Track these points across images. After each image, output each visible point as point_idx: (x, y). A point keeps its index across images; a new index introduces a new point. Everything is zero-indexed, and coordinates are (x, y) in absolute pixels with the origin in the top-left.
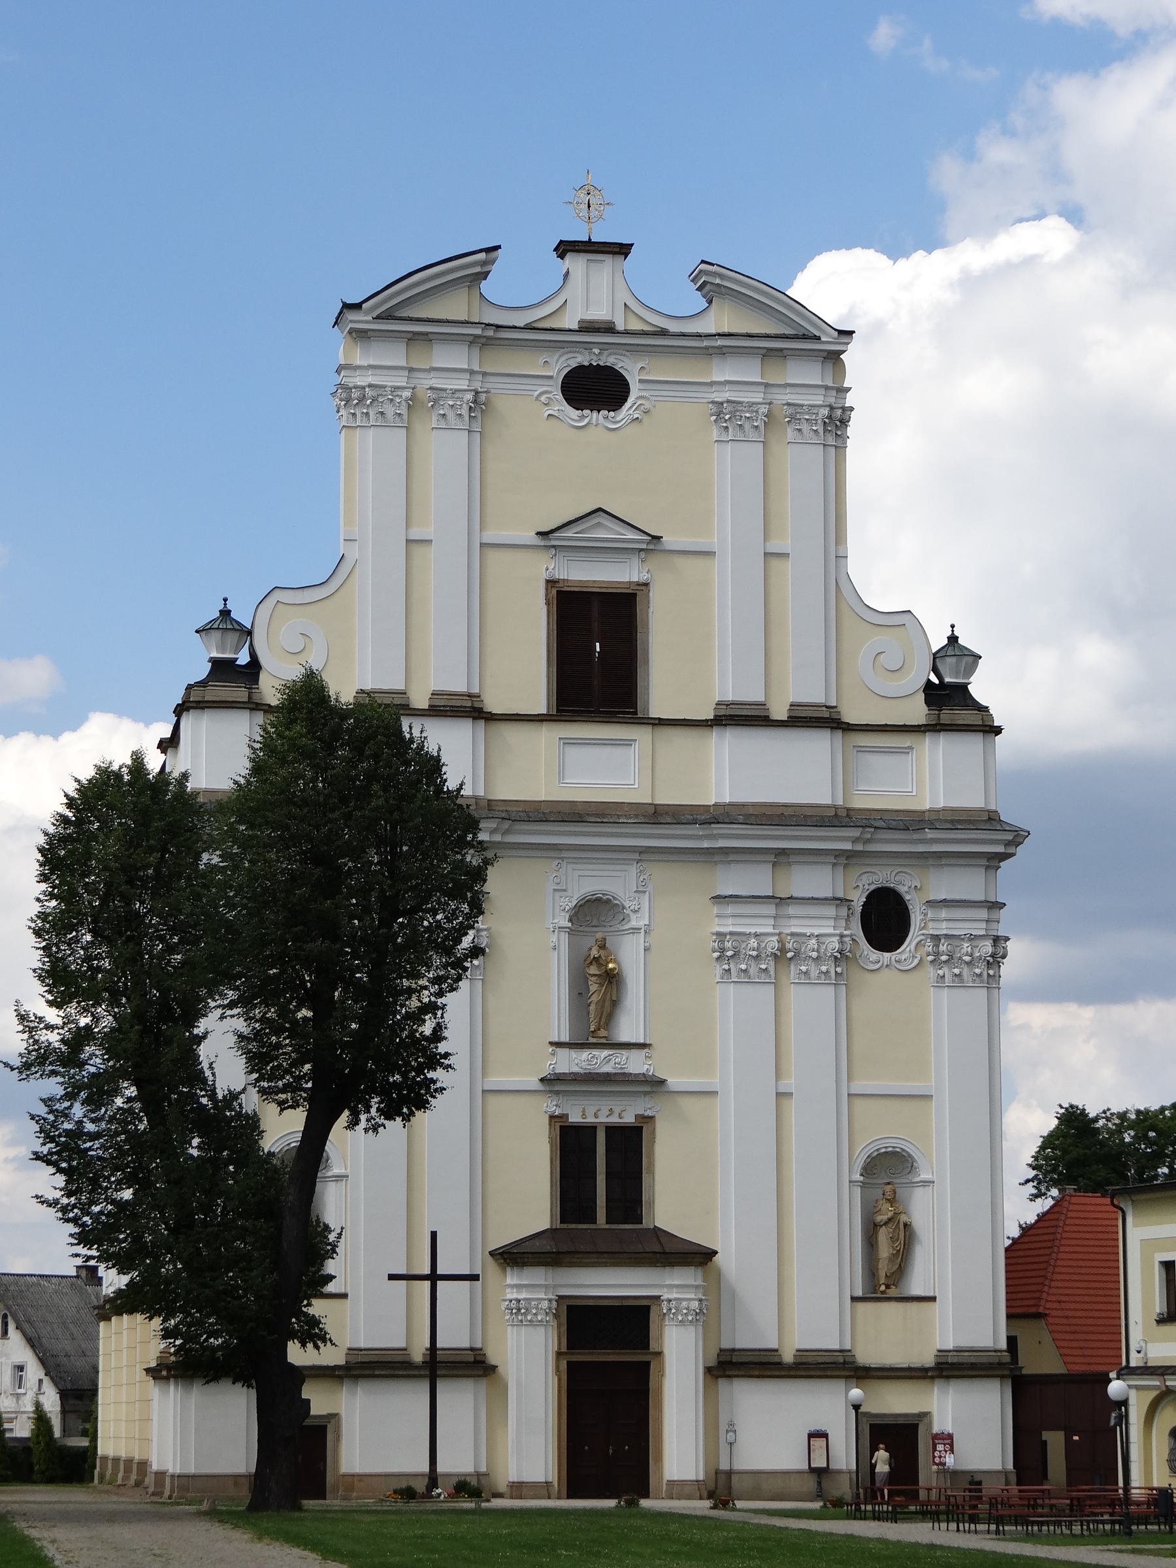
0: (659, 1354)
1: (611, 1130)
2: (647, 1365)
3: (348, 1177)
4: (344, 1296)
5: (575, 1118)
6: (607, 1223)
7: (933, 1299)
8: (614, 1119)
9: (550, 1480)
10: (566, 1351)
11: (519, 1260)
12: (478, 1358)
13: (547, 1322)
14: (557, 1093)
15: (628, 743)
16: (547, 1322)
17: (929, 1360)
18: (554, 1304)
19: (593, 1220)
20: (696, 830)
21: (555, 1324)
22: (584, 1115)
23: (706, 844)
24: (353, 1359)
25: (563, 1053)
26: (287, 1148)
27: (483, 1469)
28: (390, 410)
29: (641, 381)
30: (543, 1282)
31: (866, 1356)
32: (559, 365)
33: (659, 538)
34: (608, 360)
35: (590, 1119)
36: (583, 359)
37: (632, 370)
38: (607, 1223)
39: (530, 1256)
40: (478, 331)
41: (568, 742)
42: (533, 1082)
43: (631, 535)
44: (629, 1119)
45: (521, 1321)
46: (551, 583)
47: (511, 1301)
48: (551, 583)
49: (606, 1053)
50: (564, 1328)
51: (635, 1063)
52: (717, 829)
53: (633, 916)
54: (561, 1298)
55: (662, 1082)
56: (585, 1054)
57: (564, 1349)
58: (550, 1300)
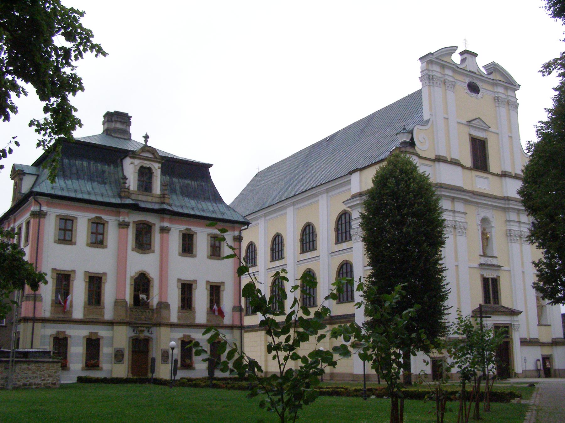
0: (512, 339)
1: (492, 279)
2: (509, 342)
5: (485, 276)
6: (493, 304)
7: (549, 325)
8: (492, 276)
14: (482, 268)
15: (487, 178)
17: (550, 341)
19: (490, 303)
20: (503, 202)
22: (487, 275)
23: (507, 206)
25: (482, 257)
28: (438, 83)
29: (482, 88)
31: (543, 339)
32: (467, 80)
33: (490, 127)
34: (475, 81)
35: (488, 276)
36: (471, 80)
37: (480, 85)
38: (493, 304)
40: (455, 67)
41: (477, 176)
42: (476, 265)
43: (485, 126)
44: (495, 277)
46: (470, 135)
48: (470, 135)
49: (490, 258)
51: (495, 262)
52: (511, 202)
53: (492, 223)
54: (494, 324)
55: (500, 267)
56: (486, 259)
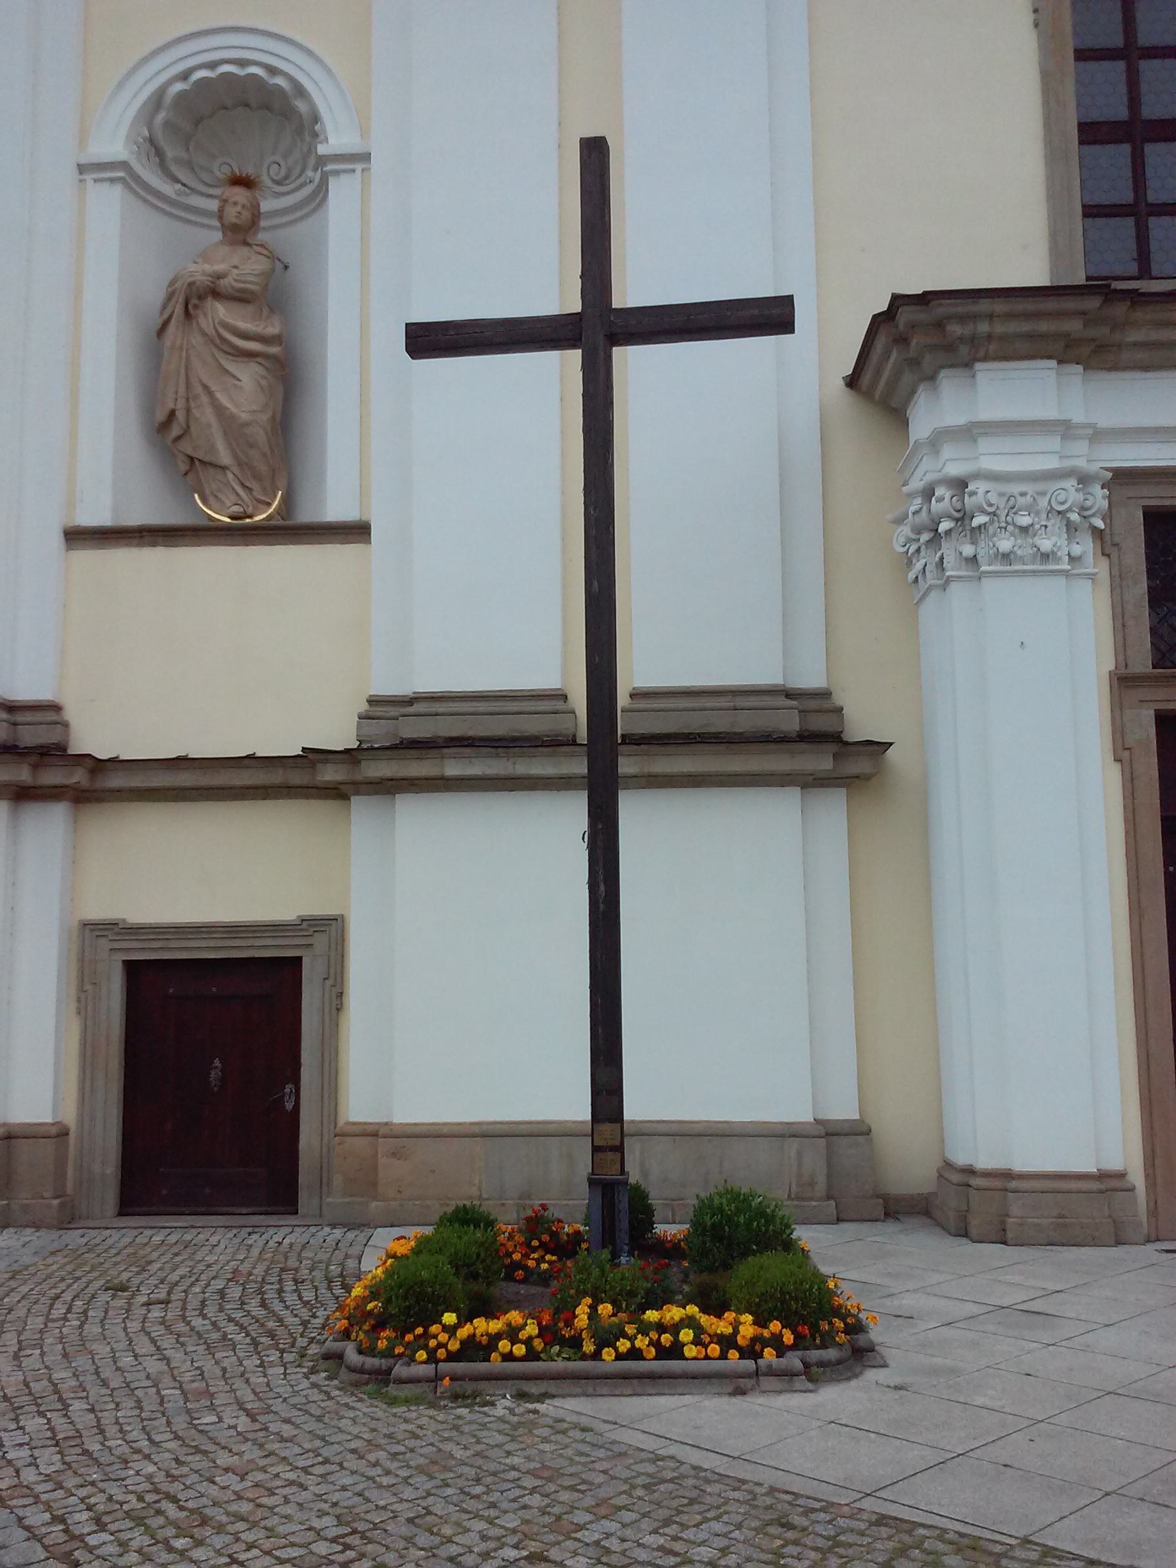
3: (365, 157)
4: (358, 532)
9: (1114, 1163)
10: (1149, 670)
11: (956, 330)
12: (819, 723)
13: (1072, 559)
16: (1072, 559)
18: (1099, 497)
21: (1102, 568)
24: (381, 733)
26: (179, 87)
27: (844, 1110)
30: (1050, 413)
39: (1000, 307)
45: (973, 560)
47: (928, 493)
50: (1140, 588)
54: (1122, 478)
57: (1142, 662)
58: (1084, 480)
